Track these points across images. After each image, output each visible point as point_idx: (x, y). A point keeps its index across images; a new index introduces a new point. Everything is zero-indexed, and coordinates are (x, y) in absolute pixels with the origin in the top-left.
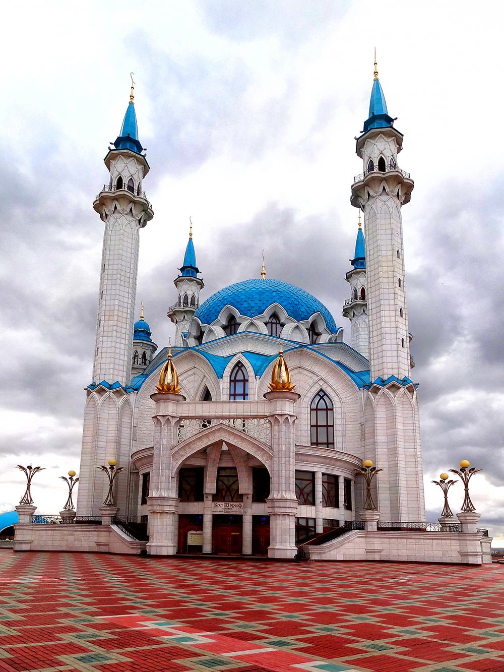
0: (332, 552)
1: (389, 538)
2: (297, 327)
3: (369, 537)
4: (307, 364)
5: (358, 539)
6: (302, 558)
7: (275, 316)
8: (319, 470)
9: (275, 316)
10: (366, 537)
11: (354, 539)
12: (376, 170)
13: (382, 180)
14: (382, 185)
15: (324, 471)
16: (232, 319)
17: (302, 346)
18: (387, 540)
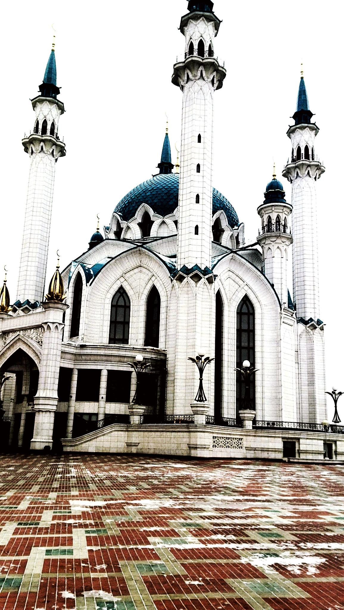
0: (84, 445)
1: (144, 431)
2: (163, 222)
3: (130, 431)
4: (146, 261)
5: (116, 432)
6: (56, 451)
7: (146, 216)
8: (105, 368)
9: (146, 216)
10: (128, 431)
11: (111, 432)
12: (195, 53)
13: (199, 64)
14: (200, 69)
15: (110, 368)
16: (118, 224)
18: (142, 433)
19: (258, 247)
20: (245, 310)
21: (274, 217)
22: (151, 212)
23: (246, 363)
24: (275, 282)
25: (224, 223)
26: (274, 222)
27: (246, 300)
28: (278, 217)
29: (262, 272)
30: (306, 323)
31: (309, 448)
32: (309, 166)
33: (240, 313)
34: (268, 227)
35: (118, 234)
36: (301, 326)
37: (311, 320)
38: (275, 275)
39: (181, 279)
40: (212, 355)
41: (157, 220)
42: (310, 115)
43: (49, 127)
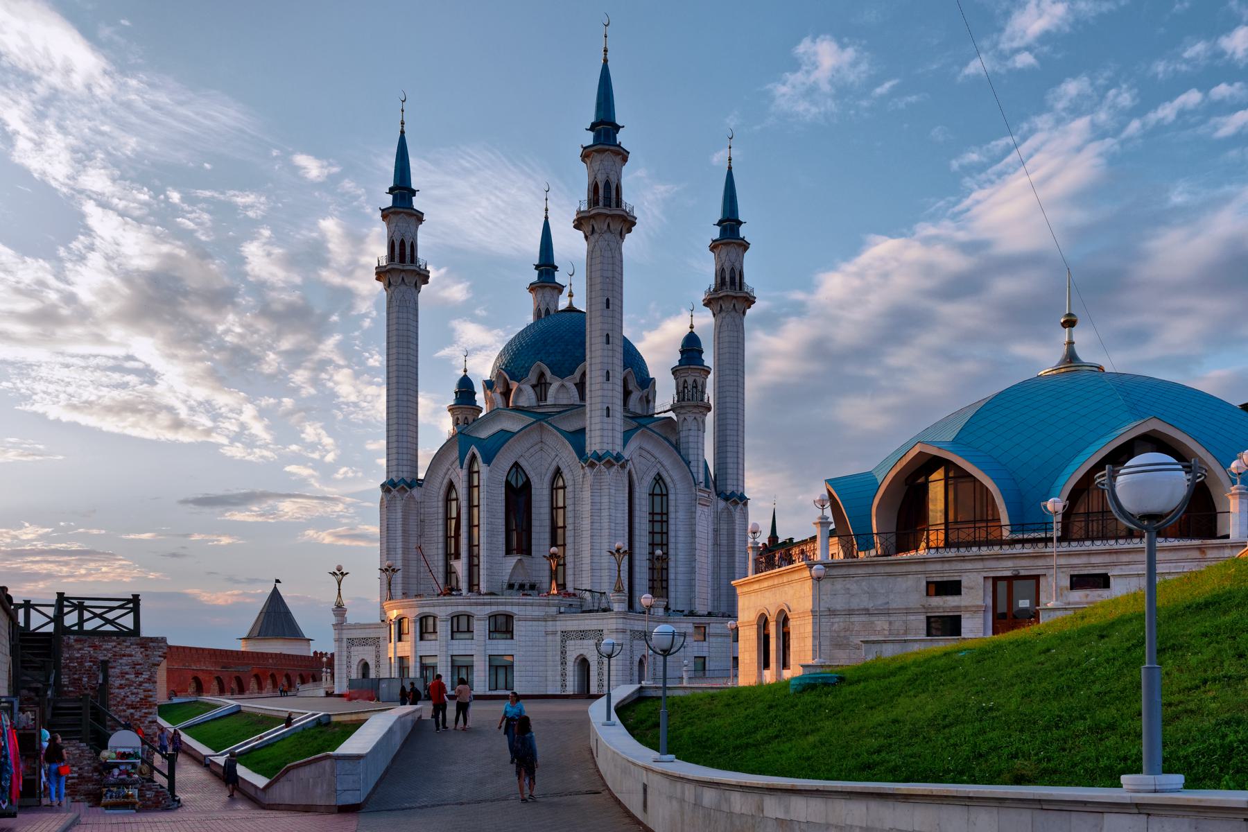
9: (542, 375)
16: (508, 385)
17: (572, 407)
19: (671, 414)
20: (657, 491)
21: (690, 381)
22: (548, 373)
23: (659, 552)
24: (691, 458)
27: (659, 479)
29: (676, 447)
31: (718, 631)
32: (735, 297)
33: (652, 495)
34: (681, 393)
35: (506, 394)
38: (691, 451)
39: (592, 465)
40: (626, 548)
41: (555, 385)
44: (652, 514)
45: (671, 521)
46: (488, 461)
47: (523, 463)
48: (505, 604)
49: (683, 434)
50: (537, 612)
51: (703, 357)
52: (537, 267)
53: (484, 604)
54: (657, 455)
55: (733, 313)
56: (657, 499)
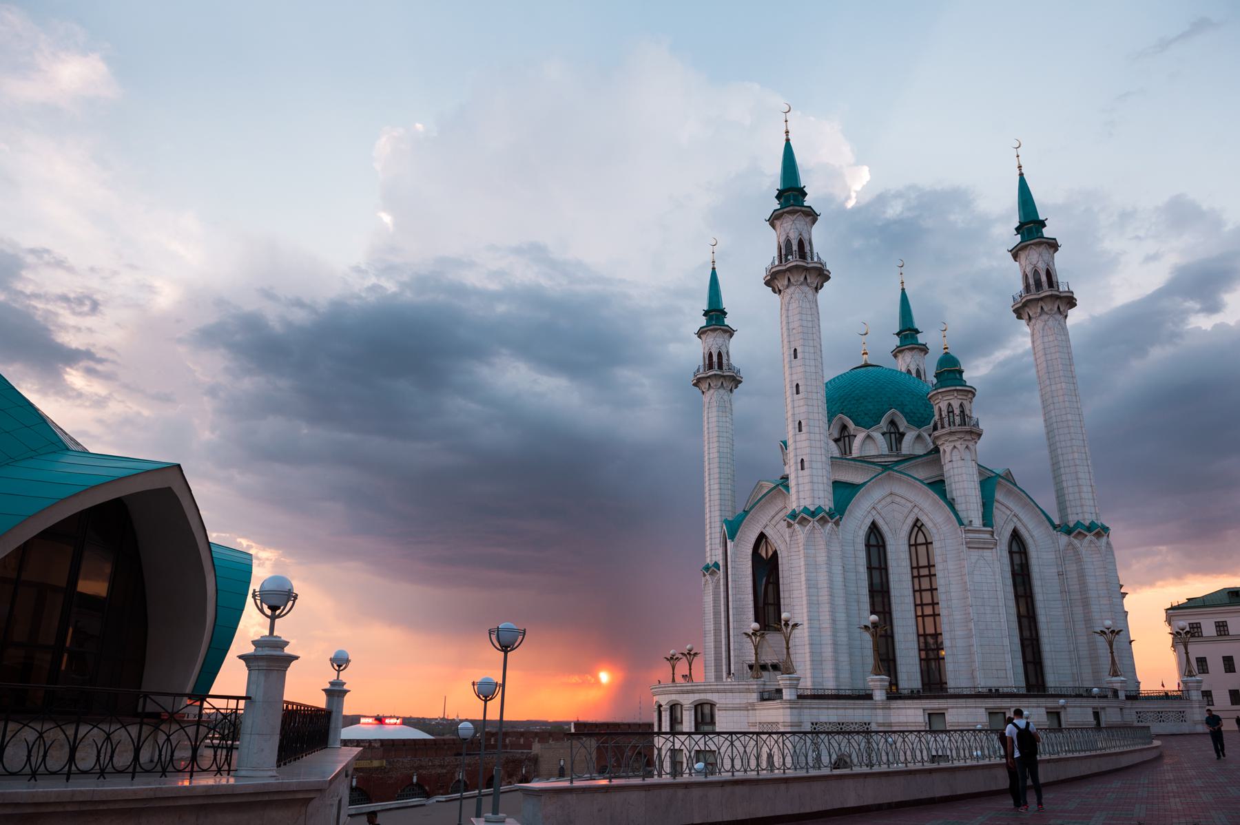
20: (921, 539)
21: (956, 404)
25: (903, 424)
26: (944, 414)
27: (918, 526)
28: (950, 405)
30: (1069, 532)
32: (1042, 299)
33: (913, 546)
36: (1064, 539)
37: (1078, 524)
42: (1042, 224)
43: (715, 359)
44: (916, 568)
45: (939, 575)
46: (732, 538)
47: (769, 532)
48: (705, 691)
49: (946, 468)
50: (738, 699)
51: (965, 376)
52: (898, 334)
53: (688, 692)
54: (912, 498)
55: (1045, 317)
56: (922, 549)
